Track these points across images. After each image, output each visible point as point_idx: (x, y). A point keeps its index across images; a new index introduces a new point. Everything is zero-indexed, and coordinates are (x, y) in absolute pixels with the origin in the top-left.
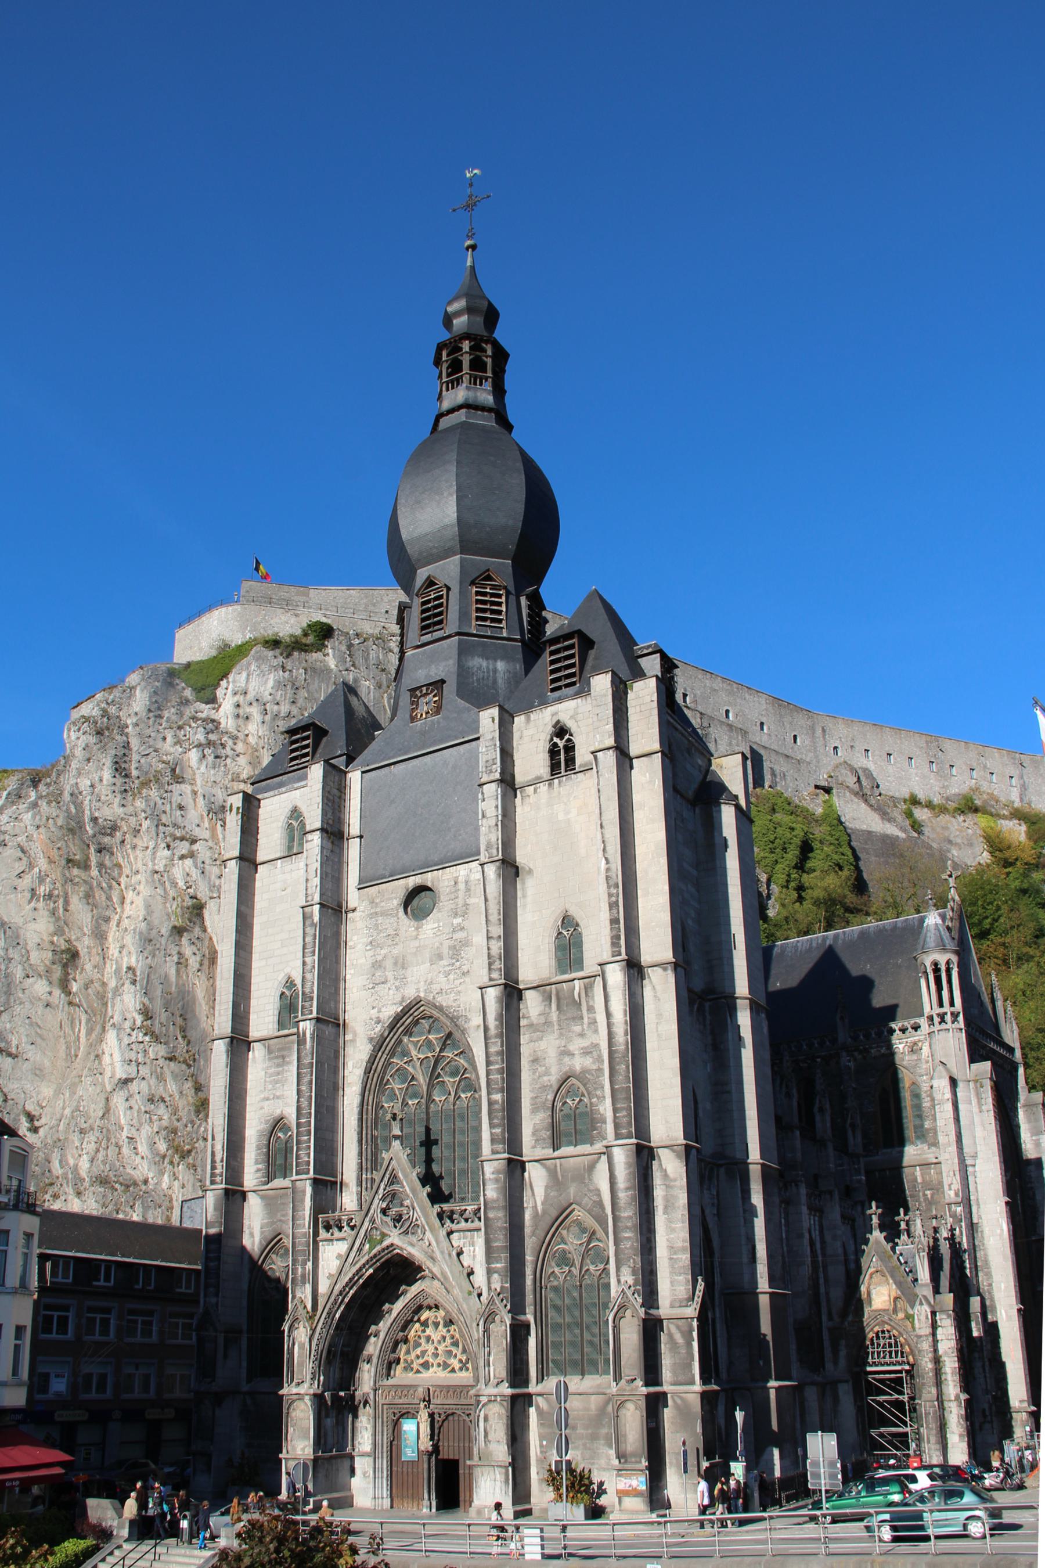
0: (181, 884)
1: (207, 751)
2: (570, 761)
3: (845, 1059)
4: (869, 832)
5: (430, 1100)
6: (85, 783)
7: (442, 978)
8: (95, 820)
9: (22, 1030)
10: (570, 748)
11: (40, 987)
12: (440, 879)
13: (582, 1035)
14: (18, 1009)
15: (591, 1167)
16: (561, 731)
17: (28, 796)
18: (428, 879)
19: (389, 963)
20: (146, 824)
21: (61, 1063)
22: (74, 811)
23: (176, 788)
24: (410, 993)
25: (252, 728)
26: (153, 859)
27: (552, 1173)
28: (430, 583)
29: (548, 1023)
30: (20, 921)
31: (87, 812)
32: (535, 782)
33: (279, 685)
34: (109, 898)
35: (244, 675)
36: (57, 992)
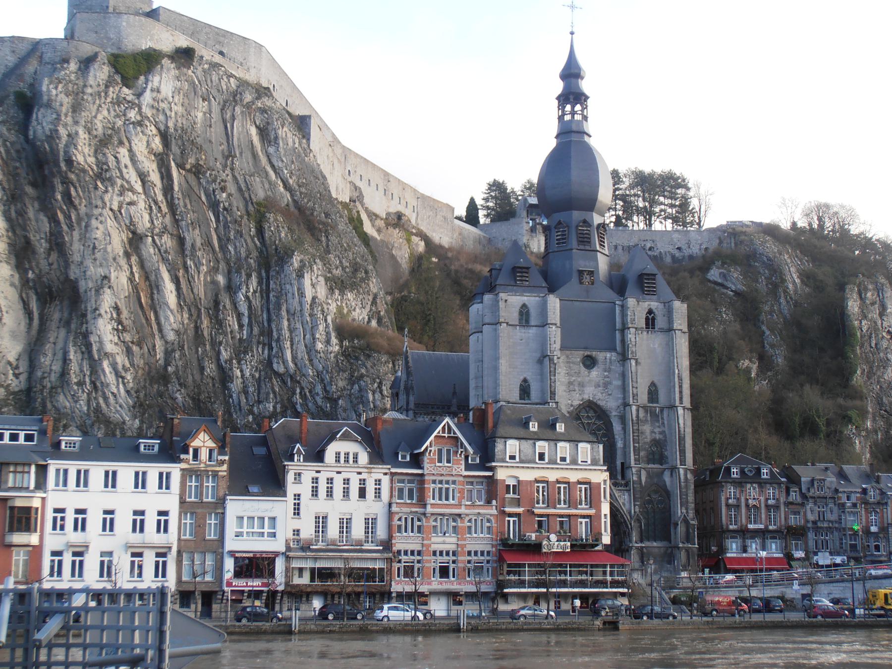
2: (653, 324)
6: (63, 132)
7: (599, 394)
8: (69, 162)
10: (653, 319)
12: (601, 356)
13: (659, 427)
15: (662, 473)
18: (594, 354)
19: (576, 383)
21: (23, 327)
24: (586, 397)
26: (111, 200)
27: (648, 473)
29: (646, 420)
31: (62, 153)
33: (177, 91)
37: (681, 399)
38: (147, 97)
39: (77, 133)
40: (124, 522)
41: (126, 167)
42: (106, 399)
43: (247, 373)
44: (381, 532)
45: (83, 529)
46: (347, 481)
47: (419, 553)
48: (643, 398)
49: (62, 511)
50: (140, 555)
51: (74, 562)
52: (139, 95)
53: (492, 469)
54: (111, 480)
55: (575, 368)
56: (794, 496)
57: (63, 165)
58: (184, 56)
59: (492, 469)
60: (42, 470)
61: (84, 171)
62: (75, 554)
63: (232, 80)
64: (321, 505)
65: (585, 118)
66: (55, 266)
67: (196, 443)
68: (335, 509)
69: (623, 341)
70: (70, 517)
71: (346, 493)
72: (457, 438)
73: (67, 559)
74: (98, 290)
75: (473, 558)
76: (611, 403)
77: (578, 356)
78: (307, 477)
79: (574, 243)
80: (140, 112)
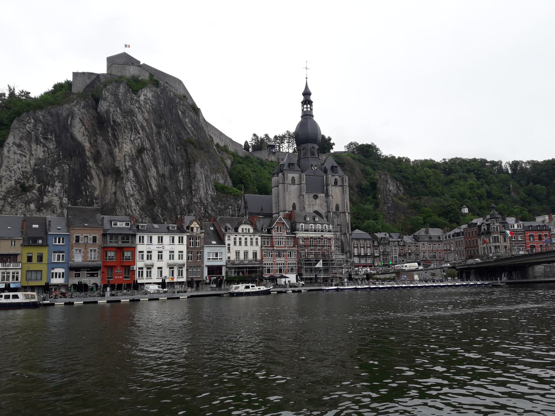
6: (112, 110)
8: (114, 121)
11: (91, 163)
16: (336, 179)
17: (80, 103)
24: (315, 209)
25: (148, 106)
33: (153, 96)
35: (146, 91)
38: (142, 98)
39: (117, 110)
40: (166, 255)
42: (132, 211)
43: (183, 203)
44: (259, 257)
45: (151, 259)
46: (246, 239)
48: (334, 210)
49: (143, 252)
50: (173, 268)
51: (147, 271)
52: (139, 97)
53: (295, 234)
54: (161, 240)
57: (111, 122)
59: (295, 234)
60: (134, 236)
62: (148, 268)
64: (238, 248)
65: (311, 109)
66: (110, 162)
67: (192, 226)
68: (242, 249)
69: (327, 190)
70: (145, 254)
71: (246, 243)
72: (283, 223)
73: (145, 270)
74: (127, 172)
75: (290, 265)
76: (323, 211)
77: (312, 195)
78: (232, 237)
79: (309, 155)
80: (139, 104)
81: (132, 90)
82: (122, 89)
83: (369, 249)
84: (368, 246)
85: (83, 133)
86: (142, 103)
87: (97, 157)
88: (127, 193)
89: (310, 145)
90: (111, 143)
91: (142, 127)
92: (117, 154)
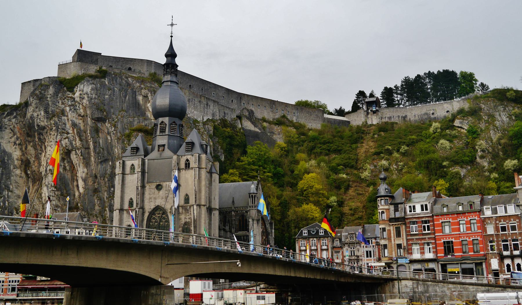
0: (64, 146)
1: (72, 108)
2: (189, 166)
3: (233, 213)
4: (250, 130)
5: (160, 224)
6: (35, 114)
8: (38, 126)
9: (13, 184)
10: (189, 164)
11: (18, 172)
14: (12, 178)
16: (187, 160)
19: (153, 198)
20: (54, 128)
22: (31, 122)
23: (63, 118)
24: (157, 204)
25: (84, 101)
26: (56, 138)
28: (162, 122)
30: (10, 151)
31: (36, 123)
32: (183, 169)
34: (41, 147)
35: (83, 85)
36: (23, 173)
37: (196, 201)
38: (77, 94)
41: (65, 124)
47: (3, 282)
52: (74, 94)
55: (153, 191)
56: (337, 243)
58: (103, 74)
61: (44, 128)
63: (130, 79)
74: (46, 176)
76: (168, 207)
77: (154, 185)
81: (67, 88)
82: (51, 90)
83: (325, 253)
84: (325, 247)
85: (15, 143)
86: (77, 99)
87: (26, 164)
88: (44, 199)
89: (161, 120)
90: (39, 148)
91: (74, 125)
92: (42, 158)
